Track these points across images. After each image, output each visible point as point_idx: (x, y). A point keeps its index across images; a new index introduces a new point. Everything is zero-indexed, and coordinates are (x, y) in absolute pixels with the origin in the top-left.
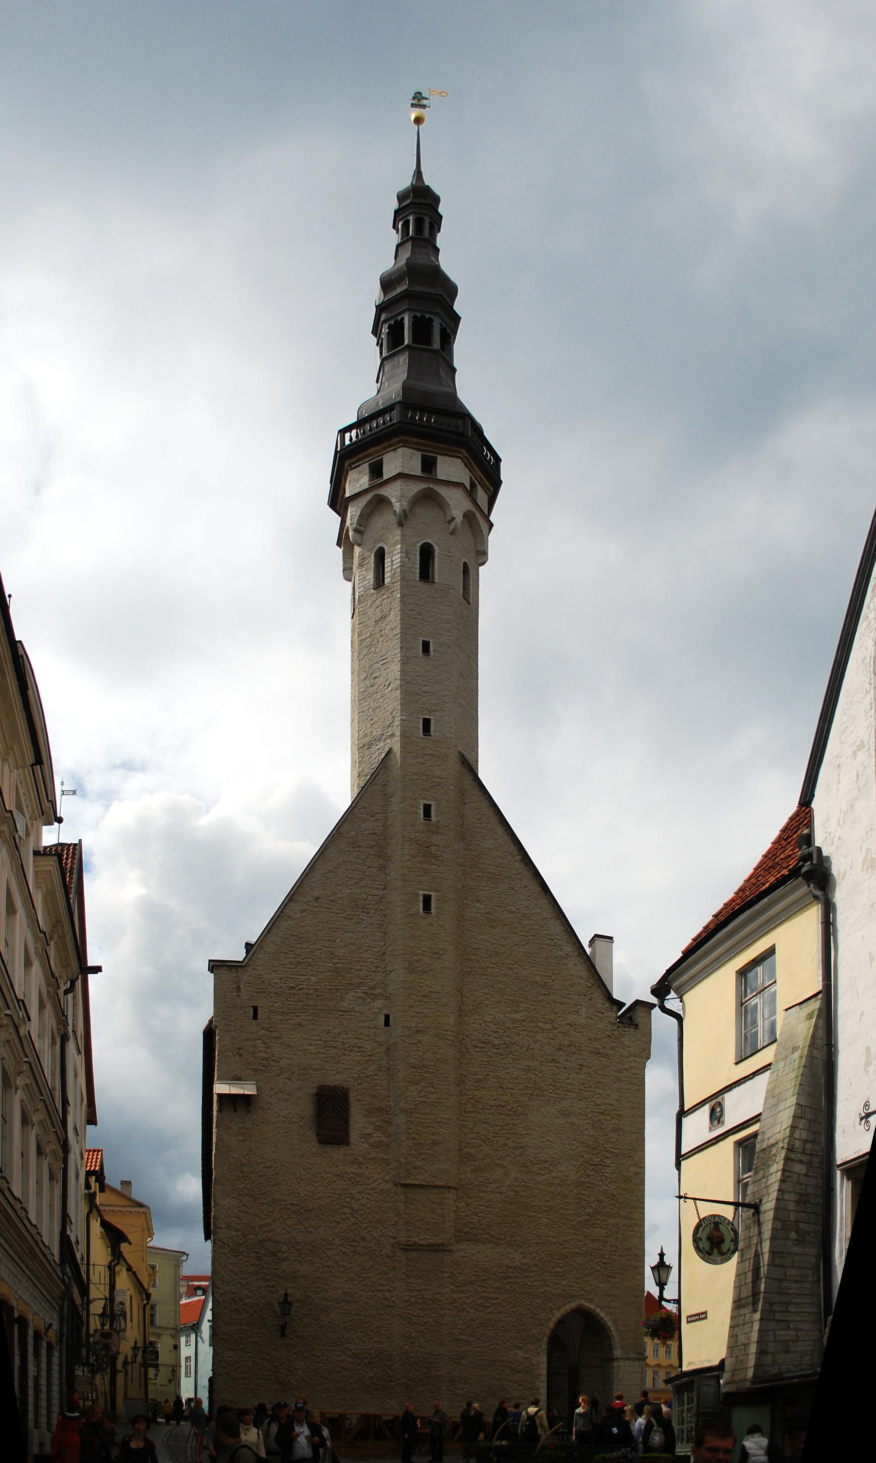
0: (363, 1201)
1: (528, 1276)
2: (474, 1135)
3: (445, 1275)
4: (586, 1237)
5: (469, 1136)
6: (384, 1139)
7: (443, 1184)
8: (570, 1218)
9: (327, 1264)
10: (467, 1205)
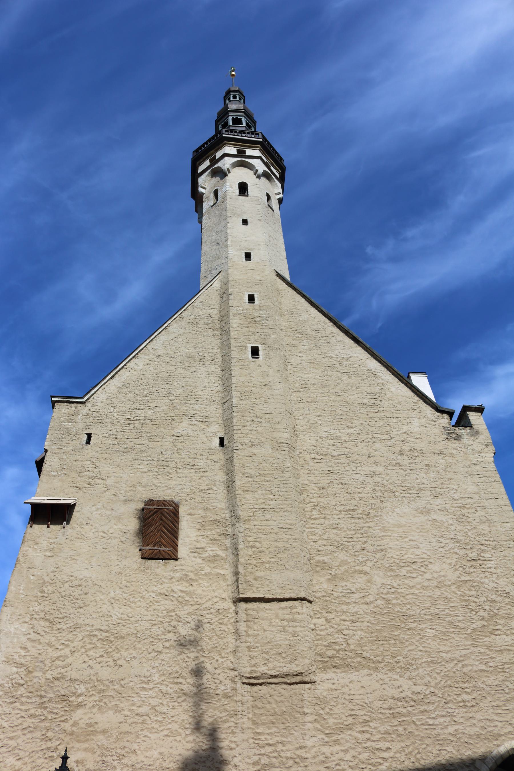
1: (425, 711)
2: (325, 542)
3: (309, 718)
4: (489, 647)
5: (320, 542)
6: (220, 553)
7: (293, 596)
8: (462, 625)
9: (140, 711)
10: (328, 621)
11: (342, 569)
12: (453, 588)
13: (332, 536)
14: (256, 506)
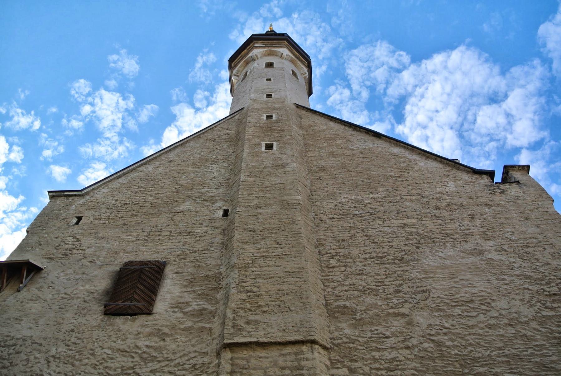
11: (371, 313)
12: (534, 324)
13: (355, 281)
14: (255, 255)
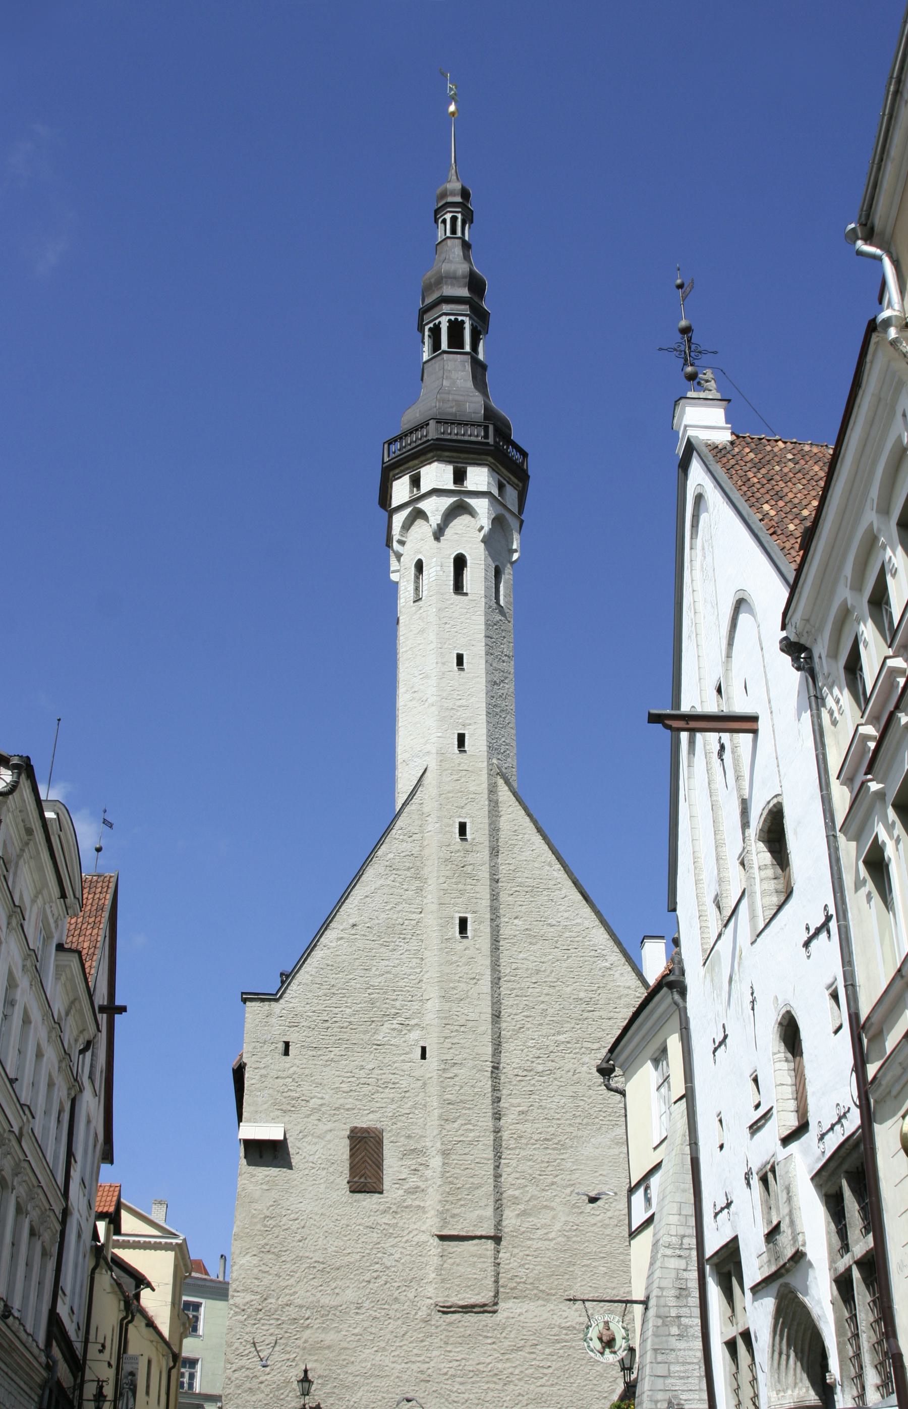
0: (397, 1256)
5: (513, 1175)
9: (356, 1331)
14: (455, 1139)
